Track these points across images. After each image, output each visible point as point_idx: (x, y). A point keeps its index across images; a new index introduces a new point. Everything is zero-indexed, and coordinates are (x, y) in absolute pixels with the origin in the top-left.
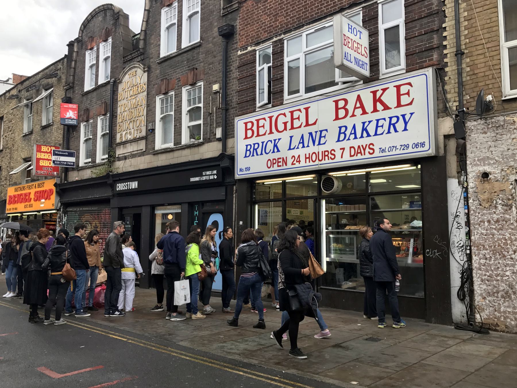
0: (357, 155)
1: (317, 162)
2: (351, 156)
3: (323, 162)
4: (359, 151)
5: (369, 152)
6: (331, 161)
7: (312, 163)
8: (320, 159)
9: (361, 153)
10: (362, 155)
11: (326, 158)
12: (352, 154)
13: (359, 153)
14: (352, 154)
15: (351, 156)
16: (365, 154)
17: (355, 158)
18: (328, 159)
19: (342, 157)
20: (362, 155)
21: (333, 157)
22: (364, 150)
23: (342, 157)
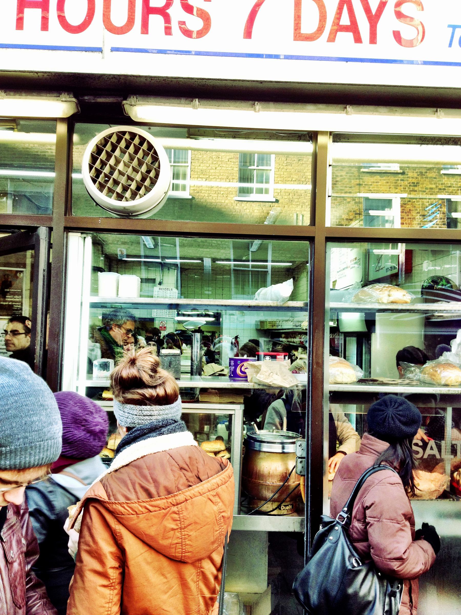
0: (332, 39)
1: (96, 33)
2: (299, 36)
3: (134, 38)
4: (345, 20)
5: (397, 36)
6: (178, 40)
7: (57, 34)
8: (119, 17)
9: (353, 28)
10: (358, 39)
11: (156, 21)
12: (309, 25)
13: (345, 29)
14: (309, 25)
15: (299, 36)
16: (373, 39)
17: (321, 46)
18: (168, 31)
19: (248, 34)
20: (358, 39)
21: (195, 23)
22: (373, 19)
23: (248, 34)
